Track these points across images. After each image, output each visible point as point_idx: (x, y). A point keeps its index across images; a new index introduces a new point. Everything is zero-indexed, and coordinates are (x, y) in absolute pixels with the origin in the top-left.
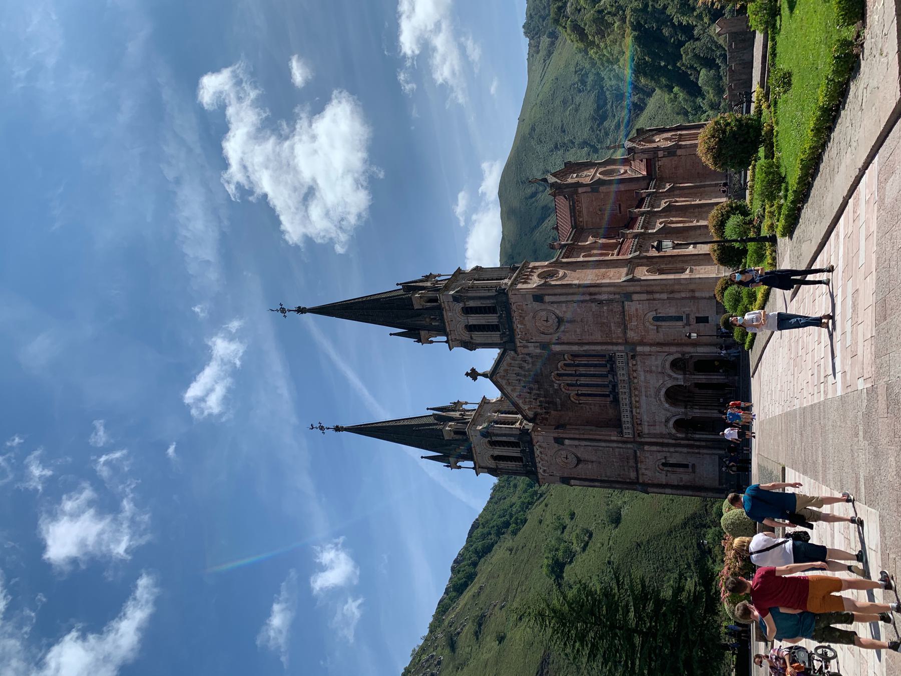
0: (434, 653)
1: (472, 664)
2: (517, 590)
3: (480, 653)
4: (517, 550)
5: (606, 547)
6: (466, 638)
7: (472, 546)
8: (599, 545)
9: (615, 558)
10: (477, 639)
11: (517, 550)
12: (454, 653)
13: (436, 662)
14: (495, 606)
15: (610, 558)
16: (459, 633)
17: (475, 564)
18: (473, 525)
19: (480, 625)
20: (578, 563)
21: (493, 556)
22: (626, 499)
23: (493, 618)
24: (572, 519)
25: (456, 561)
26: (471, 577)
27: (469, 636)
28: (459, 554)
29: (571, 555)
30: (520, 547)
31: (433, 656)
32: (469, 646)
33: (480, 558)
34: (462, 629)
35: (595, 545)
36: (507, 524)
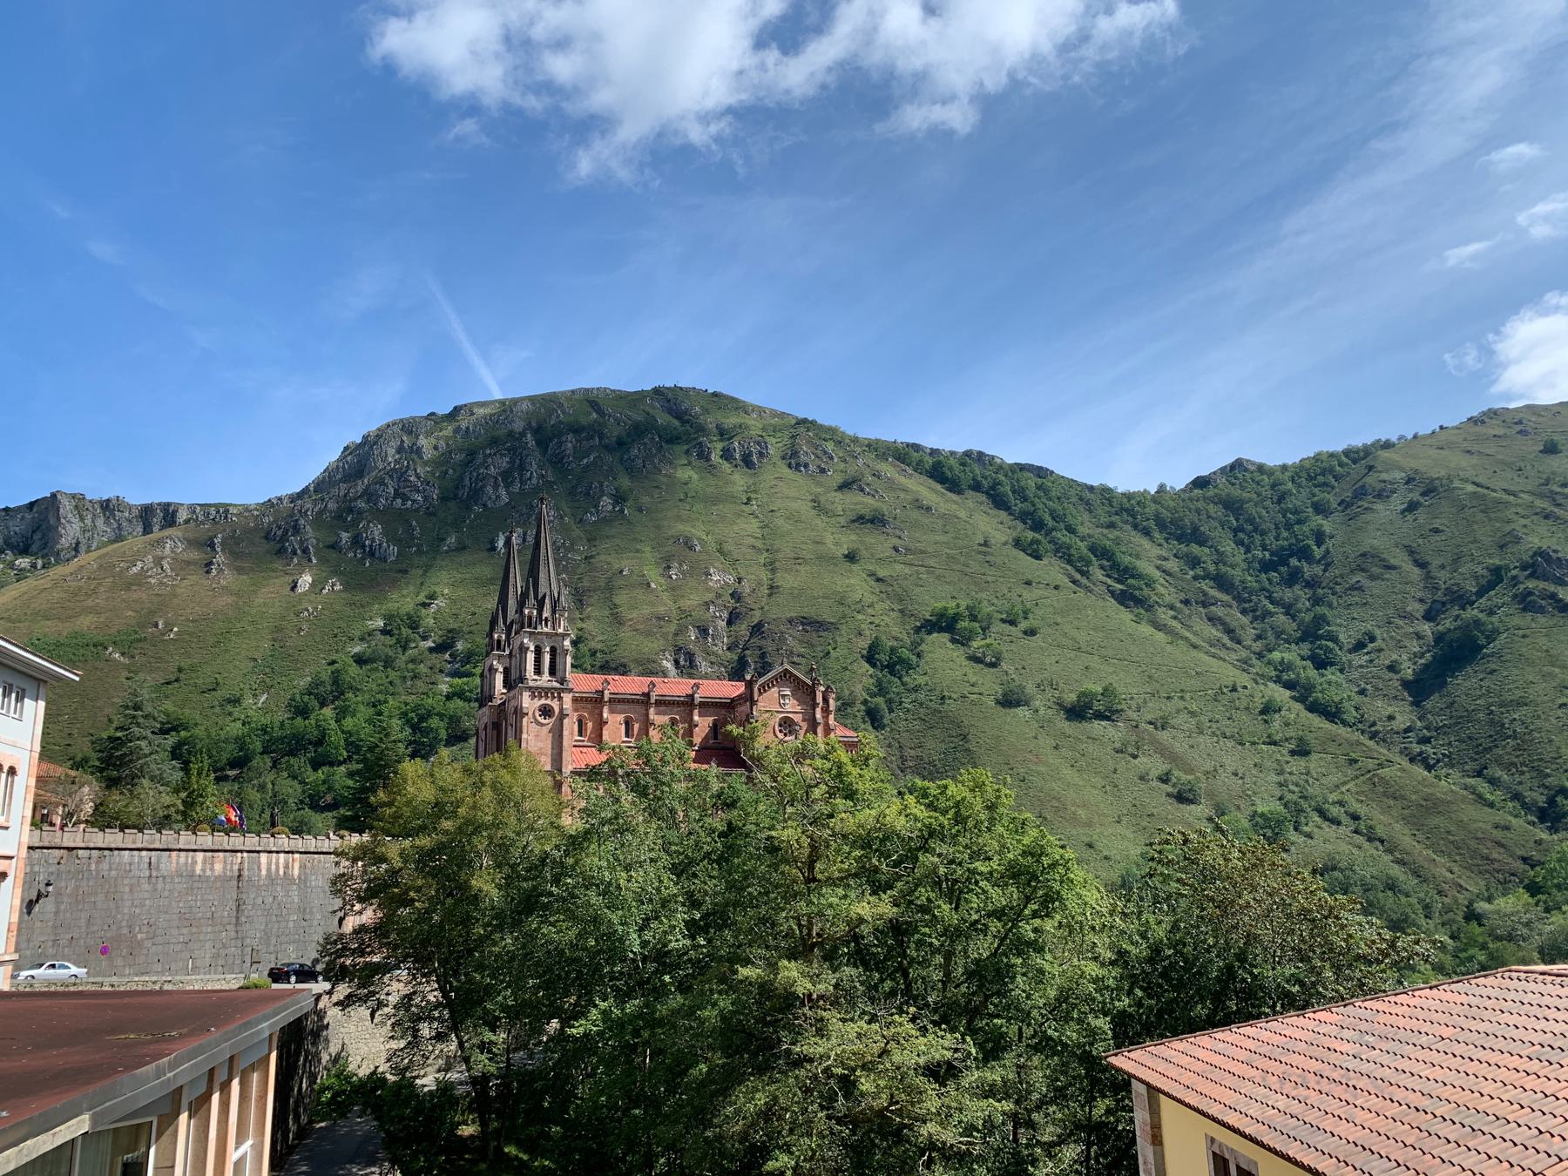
0: (836, 460)
1: (820, 523)
2: (922, 566)
3: (834, 530)
4: (985, 554)
5: (967, 689)
6: (856, 504)
7: (1006, 476)
8: (973, 680)
9: (951, 706)
10: (854, 521)
11: (985, 554)
12: (836, 490)
13: (823, 466)
14: (900, 538)
15: (950, 698)
16: (862, 490)
17: (976, 487)
18: (1041, 468)
19: (872, 521)
20: (950, 652)
21: (988, 514)
22: (1042, 712)
23: (883, 538)
24: (1025, 633)
25: (981, 454)
26: (953, 486)
27: (858, 507)
28: (993, 457)
29: (962, 640)
30: (988, 558)
31: (831, 458)
32: (843, 510)
33: (987, 493)
34: (868, 494)
35: (974, 673)
36: (1038, 526)
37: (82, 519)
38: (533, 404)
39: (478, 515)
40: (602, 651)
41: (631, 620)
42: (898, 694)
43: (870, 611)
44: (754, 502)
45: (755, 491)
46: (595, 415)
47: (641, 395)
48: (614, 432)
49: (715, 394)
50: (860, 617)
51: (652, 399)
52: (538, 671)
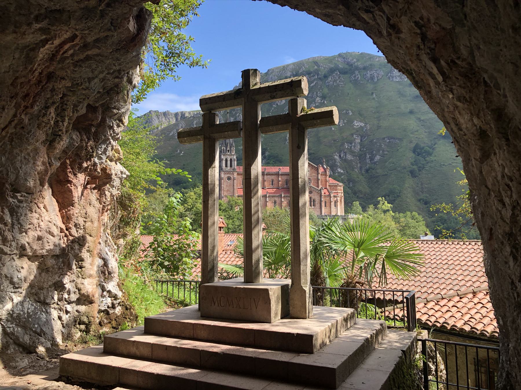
37: (158, 119)
38: (294, 66)
39: (275, 108)
40: (313, 153)
41: (324, 142)
42: (423, 164)
43: (416, 133)
44: (374, 94)
45: (376, 90)
46: (316, 67)
47: (334, 57)
48: (322, 73)
49: (362, 54)
50: (412, 136)
51: (338, 58)
52: (226, 166)
